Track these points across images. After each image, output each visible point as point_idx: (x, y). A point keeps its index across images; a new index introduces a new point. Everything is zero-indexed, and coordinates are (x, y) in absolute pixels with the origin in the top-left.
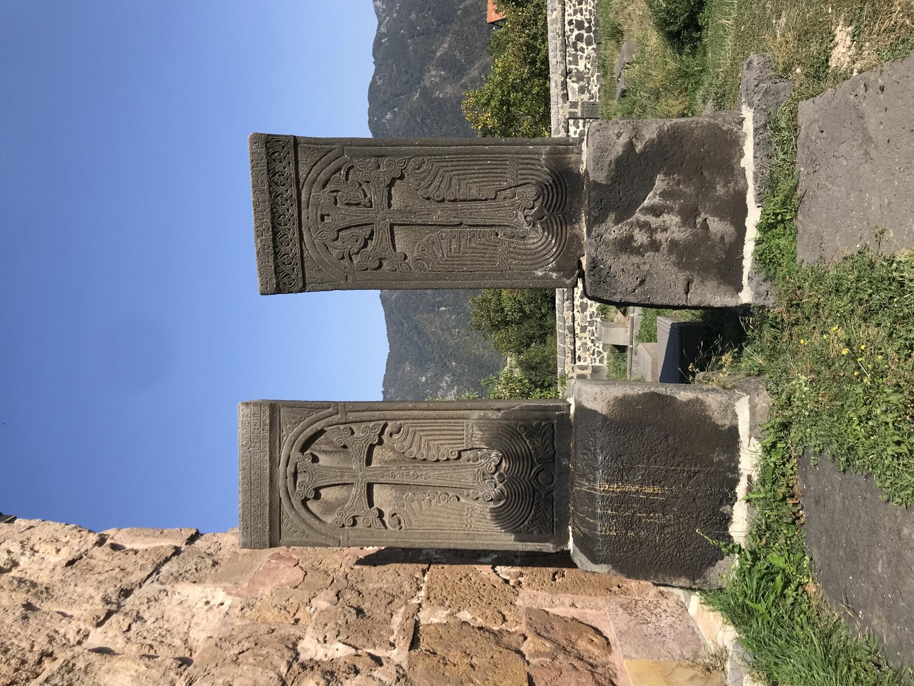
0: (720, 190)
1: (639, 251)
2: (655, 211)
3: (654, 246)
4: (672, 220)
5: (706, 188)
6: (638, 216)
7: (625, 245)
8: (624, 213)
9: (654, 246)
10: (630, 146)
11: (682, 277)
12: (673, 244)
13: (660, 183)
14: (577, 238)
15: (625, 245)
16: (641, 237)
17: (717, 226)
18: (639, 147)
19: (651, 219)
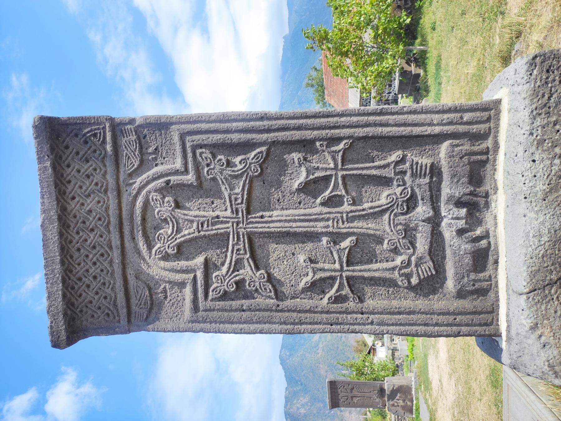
0: (409, 397)
1: (396, 406)
2: (398, 400)
3: (398, 406)
4: (401, 401)
5: (406, 396)
6: (395, 400)
7: (393, 405)
8: (393, 400)
9: (398, 406)
10: (393, 388)
11: (403, 412)
12: (401, 406)
13: (399, 395)
14: (385, 400)
15: (393, 405)
16: (396, 404)
17: (409, 403)
18: (395, 388)
19: (397, 401)
